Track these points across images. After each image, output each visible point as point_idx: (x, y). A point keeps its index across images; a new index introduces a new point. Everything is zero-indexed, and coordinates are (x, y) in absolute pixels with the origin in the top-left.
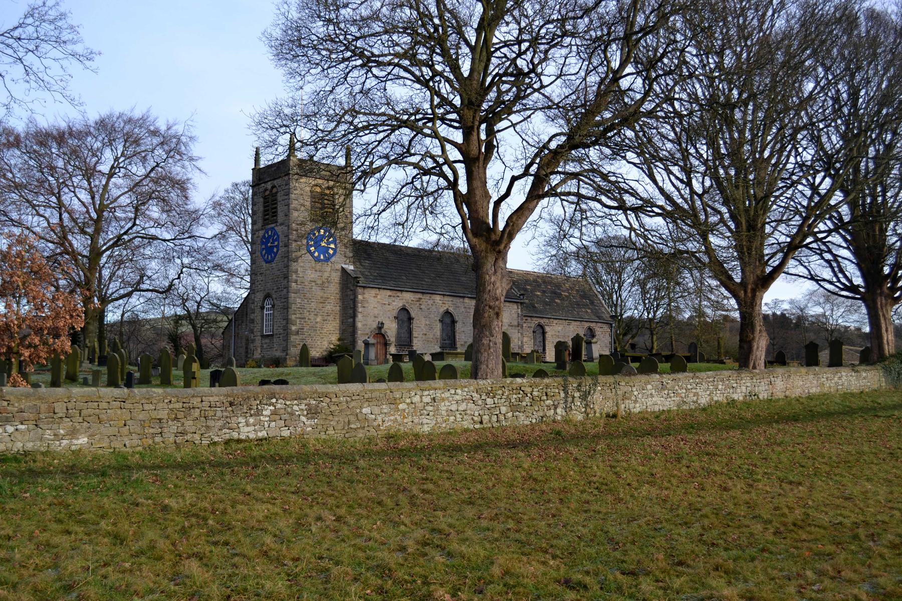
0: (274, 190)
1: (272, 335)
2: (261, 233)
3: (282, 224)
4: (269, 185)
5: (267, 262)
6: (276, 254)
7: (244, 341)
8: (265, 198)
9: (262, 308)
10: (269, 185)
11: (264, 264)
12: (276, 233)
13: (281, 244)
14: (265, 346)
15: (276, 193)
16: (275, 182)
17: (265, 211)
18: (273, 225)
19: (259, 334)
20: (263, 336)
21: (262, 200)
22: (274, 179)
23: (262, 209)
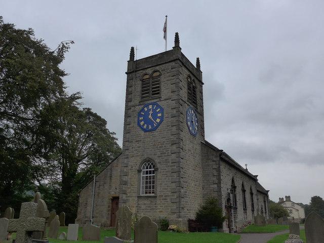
0: (155, 75)
1: (155, 197)
2: (139, 108)
4: (149, 71)
5: (145, 131)
6: (159, 124)
7: (107, 202)
8: (143, 81)
9: (139, 171)
11: (142, 133)
12: (158, 106)
13: (165, 115)
14: (143, 207)
15: (160, 75)
16: (157, 68)
17: (143, 91)
18: (155, 101)
19: (134, 195)
20: (139, 197)
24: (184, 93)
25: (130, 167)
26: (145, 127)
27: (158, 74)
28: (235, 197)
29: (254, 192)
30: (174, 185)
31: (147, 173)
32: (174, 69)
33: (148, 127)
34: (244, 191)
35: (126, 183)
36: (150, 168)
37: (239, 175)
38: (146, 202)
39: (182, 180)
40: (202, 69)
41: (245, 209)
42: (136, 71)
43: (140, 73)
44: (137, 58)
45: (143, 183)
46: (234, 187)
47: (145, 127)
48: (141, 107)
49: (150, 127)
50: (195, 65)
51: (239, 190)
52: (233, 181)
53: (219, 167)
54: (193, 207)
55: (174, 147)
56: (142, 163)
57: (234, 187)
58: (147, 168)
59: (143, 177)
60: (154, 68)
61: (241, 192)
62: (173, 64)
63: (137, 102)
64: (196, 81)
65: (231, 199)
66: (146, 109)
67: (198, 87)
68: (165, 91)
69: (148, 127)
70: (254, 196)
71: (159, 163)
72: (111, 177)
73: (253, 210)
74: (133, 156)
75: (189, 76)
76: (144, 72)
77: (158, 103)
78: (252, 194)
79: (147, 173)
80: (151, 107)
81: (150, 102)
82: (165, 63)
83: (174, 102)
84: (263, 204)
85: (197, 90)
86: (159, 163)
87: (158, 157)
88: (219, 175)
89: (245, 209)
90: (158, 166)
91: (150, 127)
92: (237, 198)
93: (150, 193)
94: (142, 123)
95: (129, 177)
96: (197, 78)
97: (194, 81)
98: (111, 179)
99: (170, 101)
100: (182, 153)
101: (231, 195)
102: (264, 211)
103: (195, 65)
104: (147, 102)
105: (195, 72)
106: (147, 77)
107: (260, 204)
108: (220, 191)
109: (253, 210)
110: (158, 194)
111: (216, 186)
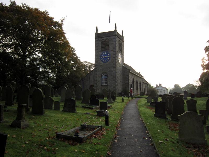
0: (107, 40)
3: (111, 51)
4: (105, 39)
8: (102, 42)
9: (101, 77)
10: (105, 39)
11: (102, 63)
13: (111, 57)
15: (109, 41)
16: (108, 38)
17: (102, 46)
18: (107, 51)
20: (102, 86)
21: (100, 43)
22: (107, 37)
23: (100, 45)
24: (117, 49)
25: (98, 75)
26: (103, 61)
27: (108, 40)
28: (134, 85)
29: (141, 83)
30: (114, 82)
31: (104, 77)
32: (115, 39)
33: (104, 61)
34: (137, 83)
35: (96, 81)
36: (105, 75)
37: (136, 77)
38: (104, 87)
39: (117, 80)
40: (124, 36)
41: (137, 90)
42: (99, 38)
43: (101, 39)
44: (98, 32)
45: (103, 81)
46: (133, 82)
47: (103, 61)
48: (101, 53)
49: (105, 61)
50: (121, 35)
51: (135, 83)
52: (133, 79)
53: (129, 75)
54: (119, 89)
55: (114, 69)
56: (102, 74)
57: (133, 82)
58: (104, 75)
59: (103, 79)
60: (107, 37)
61: (136, 83)
62: (114, 37)
63: (100, 51)
64: (122, 42)
65: (132, 86)
66: (103, 54)
67: (122, 43)
68: (111, 48)
69: (104, 61)
70: (141, 85)
71: (109, 74)
72: (90, 78)
73: (140, 90)
74: (99, 71)
75: (119, 41)
76: (102, 39)
77: (108, 52)
78: (140, 84)
79: (104, 77)
80: (105, 53)
81: (105, 51)
82: (111, 36)
83: (114, 52)
84: (145, 88)
85: (122, 45)
86: (109, 74)
87: (109, 72)
88: (129, 78)
89: (137, 90)
90: (109, 75)
91: (105, 61)
92: (135, 86)
93: (105, 84)
94: (102, 59)
95: (98, 78)
96: (122, 41)
97: (121, 42)
98: (90, 79)
99: (112, 52)
100: (117, 71)
101: (132, 85)
102: (145, 90)
103: (121, 35)
104: (104, 51)
105: (121, 38)
106: (104, 41)
107: (143, 88)
108: (129, 83)
109: (140, 90)
110: (108, 84)
111: (127, 82)
